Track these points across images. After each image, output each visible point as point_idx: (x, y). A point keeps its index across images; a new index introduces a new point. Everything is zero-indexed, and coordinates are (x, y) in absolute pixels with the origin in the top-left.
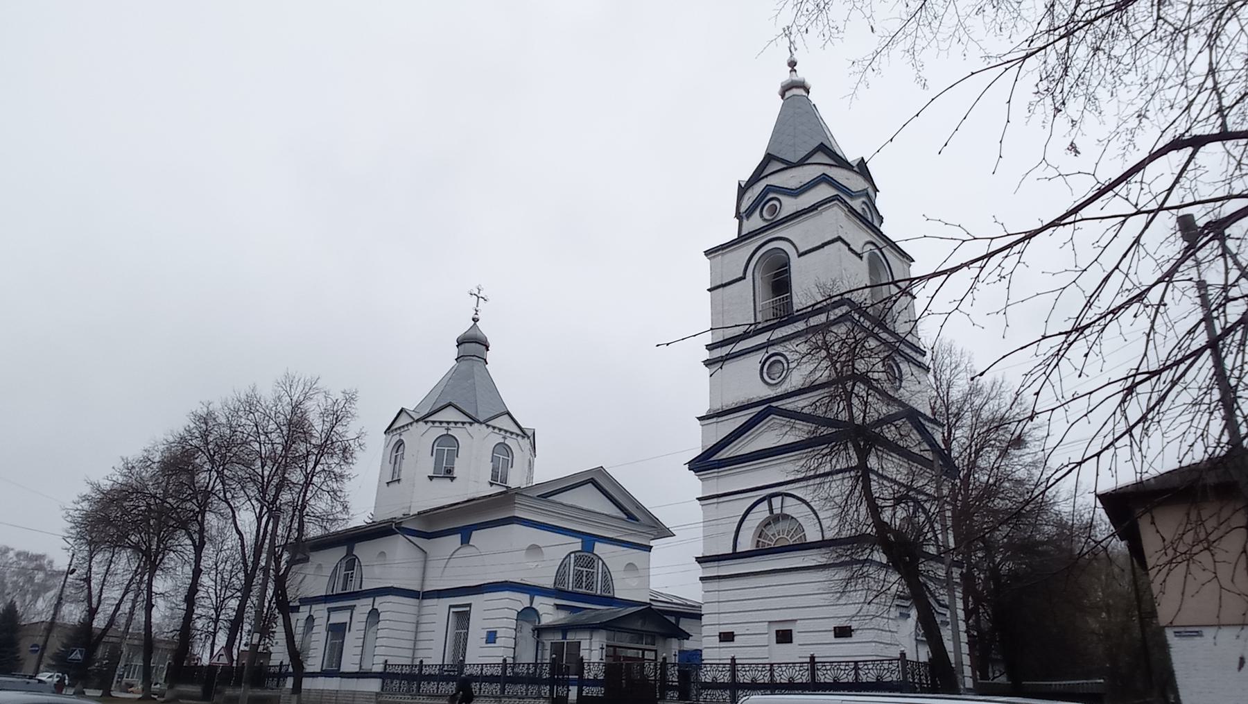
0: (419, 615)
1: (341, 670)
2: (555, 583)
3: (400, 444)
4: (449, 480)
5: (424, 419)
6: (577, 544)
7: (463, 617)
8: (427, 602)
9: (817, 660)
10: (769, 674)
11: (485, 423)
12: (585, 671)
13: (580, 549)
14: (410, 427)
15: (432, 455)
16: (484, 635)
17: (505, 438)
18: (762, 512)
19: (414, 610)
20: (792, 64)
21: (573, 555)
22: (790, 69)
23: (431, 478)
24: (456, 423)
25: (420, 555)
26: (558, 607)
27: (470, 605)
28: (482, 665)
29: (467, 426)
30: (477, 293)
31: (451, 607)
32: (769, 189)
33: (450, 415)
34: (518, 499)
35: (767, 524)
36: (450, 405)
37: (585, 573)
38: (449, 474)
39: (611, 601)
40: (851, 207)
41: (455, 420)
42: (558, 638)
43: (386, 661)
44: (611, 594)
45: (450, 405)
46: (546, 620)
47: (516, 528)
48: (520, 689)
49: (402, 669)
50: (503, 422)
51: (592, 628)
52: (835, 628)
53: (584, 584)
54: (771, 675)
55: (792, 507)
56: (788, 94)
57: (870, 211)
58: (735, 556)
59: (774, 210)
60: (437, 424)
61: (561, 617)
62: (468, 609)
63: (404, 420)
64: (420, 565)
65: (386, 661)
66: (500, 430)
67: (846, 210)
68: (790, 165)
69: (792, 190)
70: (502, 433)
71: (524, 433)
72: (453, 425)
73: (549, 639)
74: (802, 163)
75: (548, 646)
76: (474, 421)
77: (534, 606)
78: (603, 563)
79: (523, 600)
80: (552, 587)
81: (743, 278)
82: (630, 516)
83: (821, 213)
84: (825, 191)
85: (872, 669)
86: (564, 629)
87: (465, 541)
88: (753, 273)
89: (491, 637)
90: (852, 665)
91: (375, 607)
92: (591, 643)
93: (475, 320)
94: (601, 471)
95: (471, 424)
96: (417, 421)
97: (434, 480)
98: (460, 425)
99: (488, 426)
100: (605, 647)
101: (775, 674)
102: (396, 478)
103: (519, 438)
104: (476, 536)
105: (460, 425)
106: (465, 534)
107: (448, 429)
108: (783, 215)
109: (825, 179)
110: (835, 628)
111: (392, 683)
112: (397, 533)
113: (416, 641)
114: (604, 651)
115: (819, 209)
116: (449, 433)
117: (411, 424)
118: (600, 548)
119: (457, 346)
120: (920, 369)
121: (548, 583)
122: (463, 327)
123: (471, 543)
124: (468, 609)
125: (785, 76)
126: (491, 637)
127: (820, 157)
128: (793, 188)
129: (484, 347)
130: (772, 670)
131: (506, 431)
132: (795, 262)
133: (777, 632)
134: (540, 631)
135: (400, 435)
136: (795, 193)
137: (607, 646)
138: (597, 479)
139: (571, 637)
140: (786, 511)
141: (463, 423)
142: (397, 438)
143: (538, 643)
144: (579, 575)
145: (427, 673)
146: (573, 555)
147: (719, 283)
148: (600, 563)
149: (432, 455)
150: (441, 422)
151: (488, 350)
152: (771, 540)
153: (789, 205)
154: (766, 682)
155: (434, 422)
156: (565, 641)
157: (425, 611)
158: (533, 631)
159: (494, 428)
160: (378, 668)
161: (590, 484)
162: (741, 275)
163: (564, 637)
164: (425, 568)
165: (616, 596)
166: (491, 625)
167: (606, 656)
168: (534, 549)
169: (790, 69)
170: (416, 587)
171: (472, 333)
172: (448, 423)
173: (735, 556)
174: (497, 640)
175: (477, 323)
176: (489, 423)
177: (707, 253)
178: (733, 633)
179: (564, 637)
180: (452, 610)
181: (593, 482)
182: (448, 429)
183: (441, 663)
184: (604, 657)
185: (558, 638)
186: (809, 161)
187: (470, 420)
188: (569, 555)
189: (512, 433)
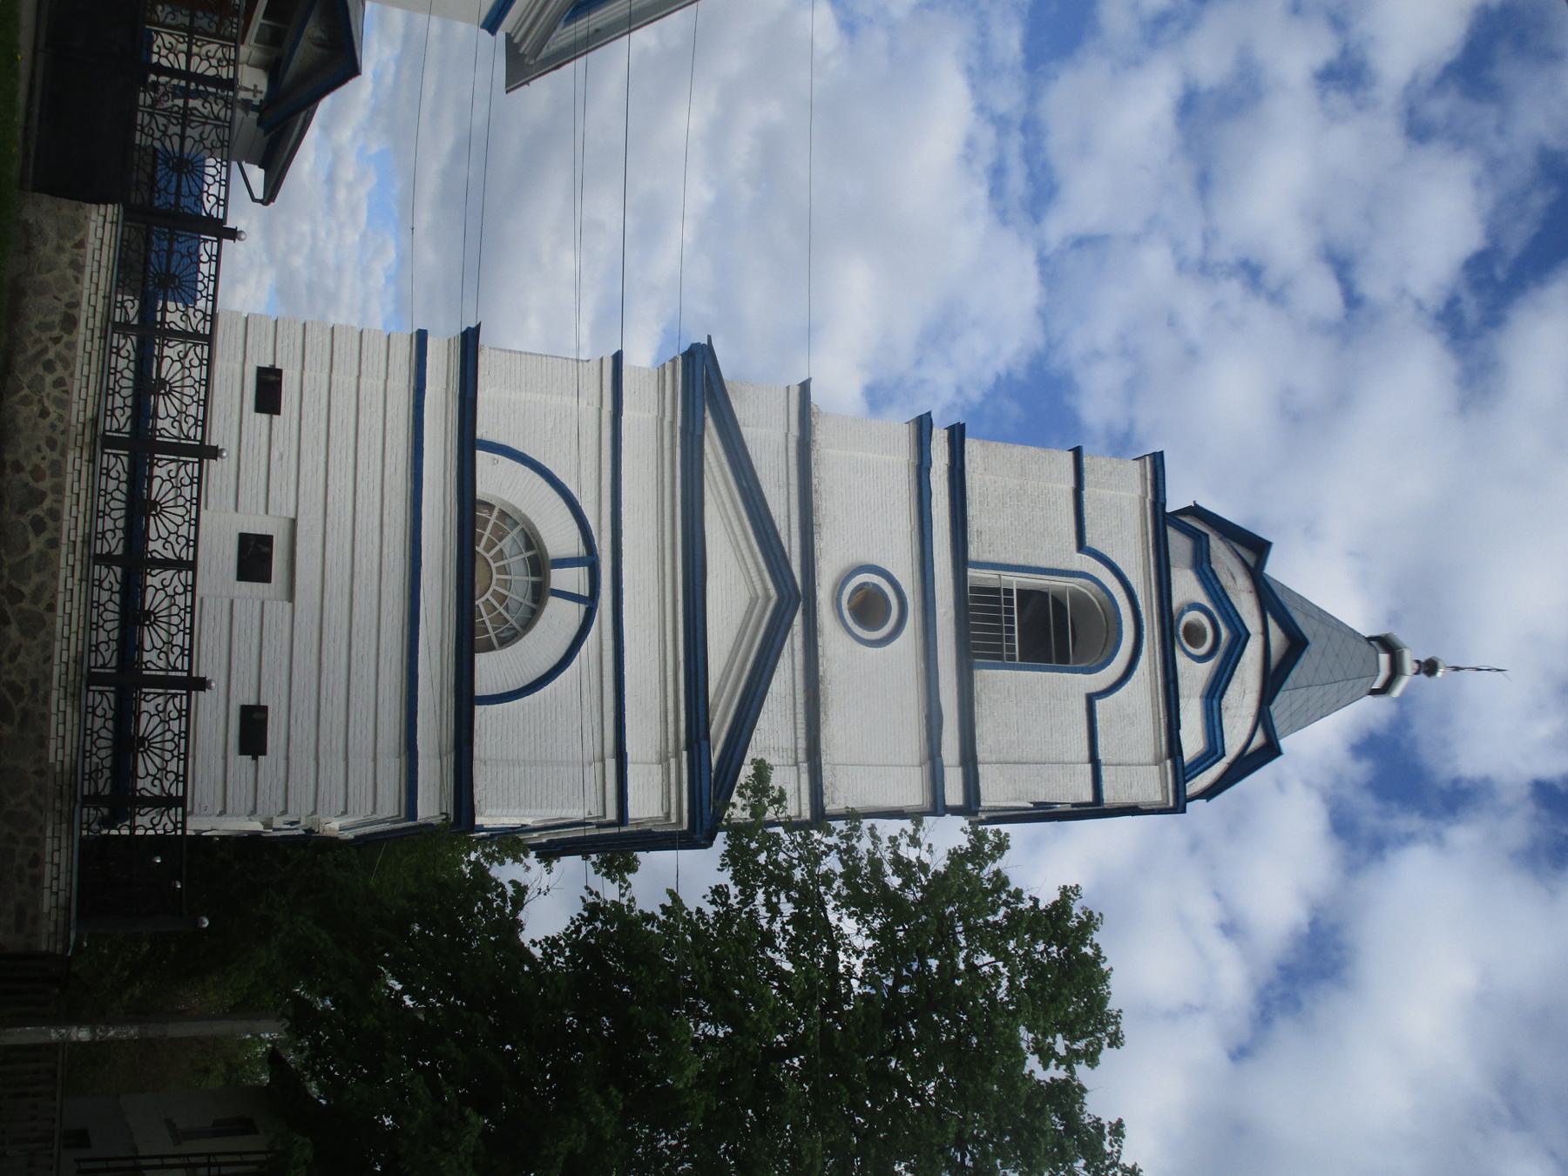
10: (170, 555)
18: (560, 537)
35: (531, 540)
52: (265, 709)
55: (560, 618)
58: (468, 443)
90: (176, 790)
110: (265, 709)
133: (267, 540)
140: (553, 604)
152: (490, 546)
173: (468, 443)
178: (278, 413)
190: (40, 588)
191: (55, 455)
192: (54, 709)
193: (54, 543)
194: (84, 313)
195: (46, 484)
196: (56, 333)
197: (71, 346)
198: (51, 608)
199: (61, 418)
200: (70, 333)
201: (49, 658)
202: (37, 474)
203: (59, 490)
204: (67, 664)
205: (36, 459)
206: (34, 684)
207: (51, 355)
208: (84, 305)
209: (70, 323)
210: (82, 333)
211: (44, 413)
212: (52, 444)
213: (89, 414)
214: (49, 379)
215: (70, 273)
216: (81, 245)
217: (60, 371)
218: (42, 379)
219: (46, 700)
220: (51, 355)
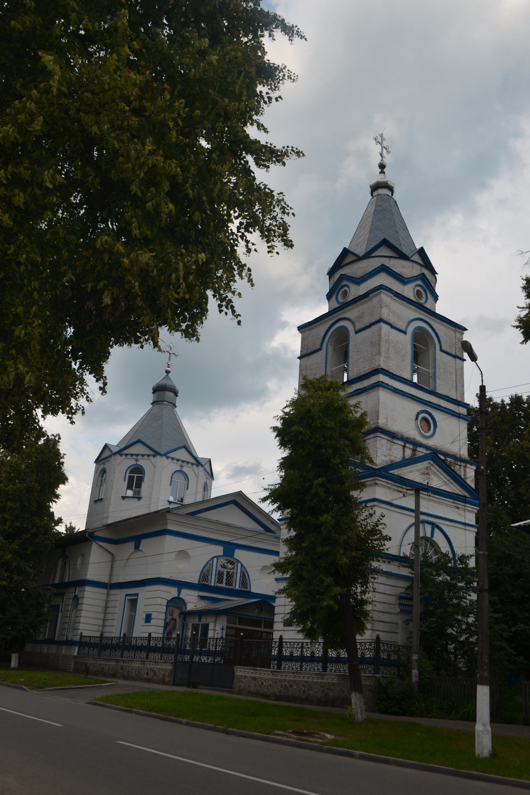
0: (107, 601)
1: (56, 639)
2: (199, 581)
3: (104, 471)
4: (136, 500)
5: (120, 452)
6: (219, 550)
7: (134, 603)
8: (113, 592)
9: (284, 641)
10: (300, 650)
11: (166, 455)
12: (284, 649)
13: (222, 554)
14: (110, 459)
15: (125, 480)
16: (144, 617)
17: (182, 466)
19: (104, 597)
20: (382, 166)
21: (215, 559)
22: (380, 170)
23: (124, 498)
24: (143, 455)
25: (108, 558)
26: (202, 598)
27: (137, 595)
28: (137, 638)
29: (151, 458)
30: (169, 350)
31: (127, 595)
32: (343, 277)
33: (139, 449)
34: (169, 516)
36: (139, 441)
37: (225, 573)
38: (138, 497)
39: (249, 594)
40: (396, 292)
41: (143, 453)
42: (196, 621)
43: (81, 634)
44: (249, 590)
45: (139, 441)
46: (190, 607)
47: (168, 538)
48: (158, 656)
49: (90, 640)
50: (182, 454)
51: (216, 614)
53: (224, 581)
54: (301, 651)
56: (375, 194)
57: (425, 292)
59: (345, 294)
60: (129, 457)
61: (202, 605)
62: (136, 597)
63: (107, 454)
64: (109, 565)
65: (81, 634)
66: (178, 460)
67: (392, 296)
68: (360, 259)
69: (357, 279)
70: (180, 463)
71: (198, 462)
72: (140, 457)
73: (192, 621)
74: (368, 255)
75: (190, 627)
76: (156, 454)
77: (182, 596)
78: (242, 565)
79: (173, 592)
80: (197, 582)
81: (320, 349)
82: (267, 529)
83: (371, 299)
84: (382, 279)
85: (289, 647)
86: (200, 613)
87: (137, 547)
88: (327, 345)
89: (148, 618)
91: (76, 594)
92: (215, 625)
93: (168, 372)
94: (240, 494)
95: (154, 456)
96: (115, 454)
97: (126, 500)
98: (146, 457)
99: (168, 458)
100: (225, 627)
101: (304, 650)
102: (100, 498)
103: (194, 467)
104: (144, 543)
105: (146, 457)
106: (137, 540)
107: (137, 460)
108: (351, 297)
109: (384, 269)
111: (84, 649)
112: (90, 540)
113: (104, 620)
114: (224, 631)
115: (371, 296)
116: (138, 463)
117: (111, 456)
118: (239, 554)
119: (153, 393)
120: (461, 420)
121: (195, 579)
122: (158, 378)
123: (140, 548)
124: (136, 597)
125: (376, 177)
126: (148, 618)
127: (384, 251)
128: (358, 277)
129: (172, 394)
130: (302, 647)
131: (183, 461)
132: (354, 339)
134: (186, 615)
135: (104, 464)
136: (359, 281)
137: (227, 627)
138: (237, 500)
139: (204, 621)
141: (149, 456)
142: (101, 467)
143: (184, 624)
144: (220, 575)
145: (93, 642)
146: (215, 559)
147: (305, 352)
148: (239, 565)
149: (125, 480)
150: (132, 455)
151: (177, 396)
153: (355, 291)
154: (299, 655)
155: (126, 455)
156: (200, 623)
157: (111, 598)
158: (180, 615)
159: (173, 459)
160: (78, 638)
161: (232, 506)
162: (318, 347)
163: (200, 620)
164: (112, 567)
165: (252, 591)
166: (149, 610)
167: (226, 635)
168: (183, 554)
169: (380, 170)
170: (105, 579)
171: (164, 382)
172: (137, 455)
174: (152, 621)
175: (169, 374)
176: (169, 455)
177: (301, 328)
179: (200, 620)
180: (128, 598)
181: (234, 502)
182: (137, 460)
183: (119, 636)
184: (224, 636)
185: (196, 621)
186: (373, 255)
187: (153, 453)
188: (213, 558)
189: (188, 463)
190: (304, 686)
191: (278, 681)
192: (327, 681)
193: (295, 681)
194: (253, 675)
195: (283, 684)
196: (257, 682)
197: (259, 678)
198: (307, 682)
199: (271, 680)
200: (257, 679)
201: (317, 683)
202: (282, 687)
203: (285, 680)
204: (318, 678)
205: (279, 687)
206: (322, 686)
207: (260, 683)
208: (252, 675)
209: (255, 679)
210: (257, 676)
211: (270, 685)
212: (276, 683)
213: (270, 673)
214: (265, 684)
215: (246, 679)
216: (241, 676)
217: (263, 681)
218: (265, 686)
219: (325, 683)
220: (260, 683)
